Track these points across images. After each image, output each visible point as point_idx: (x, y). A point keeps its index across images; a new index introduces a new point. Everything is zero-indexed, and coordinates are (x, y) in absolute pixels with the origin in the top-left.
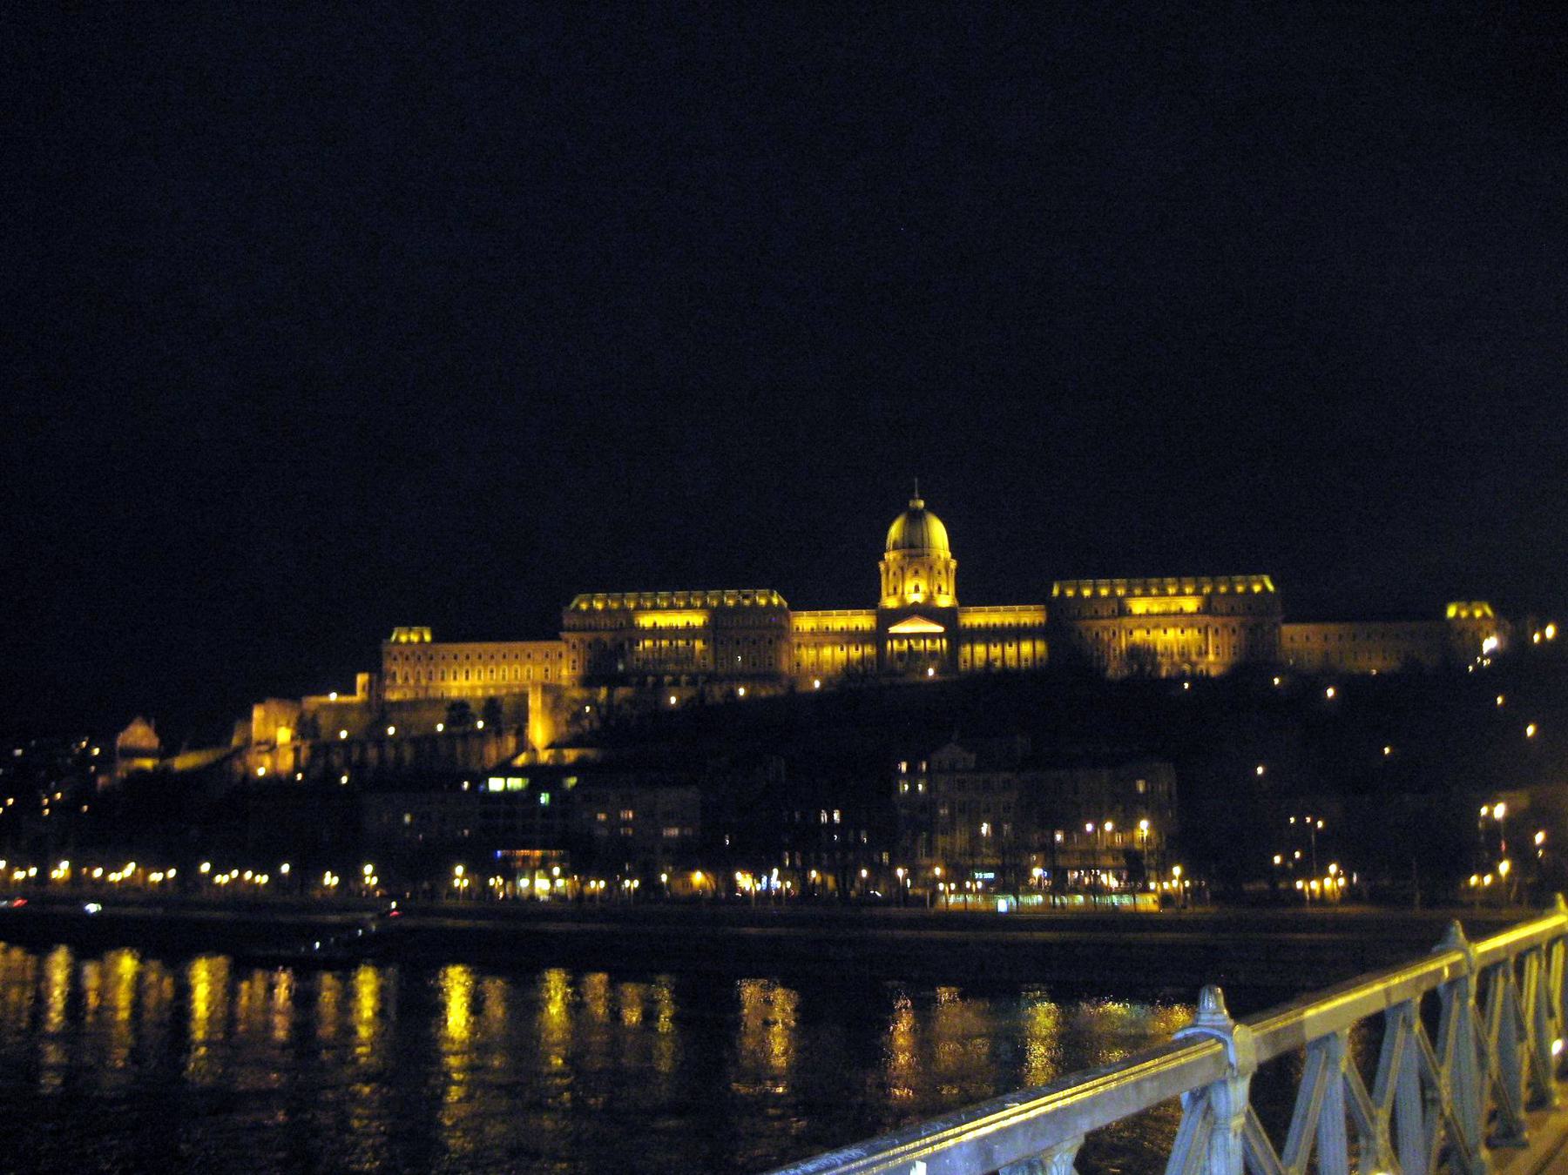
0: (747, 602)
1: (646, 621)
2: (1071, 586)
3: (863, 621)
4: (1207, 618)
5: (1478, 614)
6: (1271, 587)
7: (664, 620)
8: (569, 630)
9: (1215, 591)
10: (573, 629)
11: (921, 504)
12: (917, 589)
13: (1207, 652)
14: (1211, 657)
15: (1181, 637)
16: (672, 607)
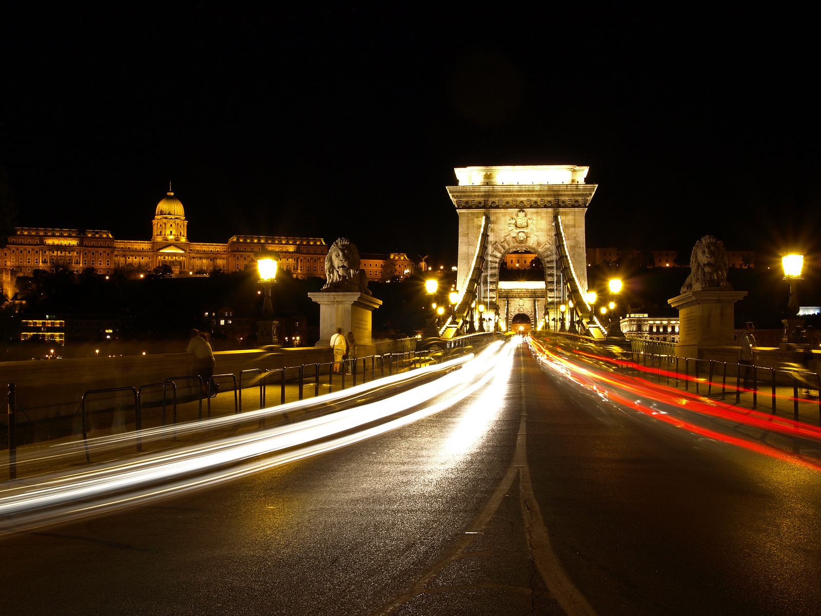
0: (97, 236)
1: (50, 241)
2: (242, 238)
3: (144, 245)
4: (298, 255)
5: (402, 258)
6: (324, 243)
7: (56, 242)
8: (11, 244)
9: (301, 244)
10: (13, 244)
11: (172, 194)
12: (171, 232)
13: (297, 269)
14: (299, 271)
15: (287, 262)
16: (61, 236)
